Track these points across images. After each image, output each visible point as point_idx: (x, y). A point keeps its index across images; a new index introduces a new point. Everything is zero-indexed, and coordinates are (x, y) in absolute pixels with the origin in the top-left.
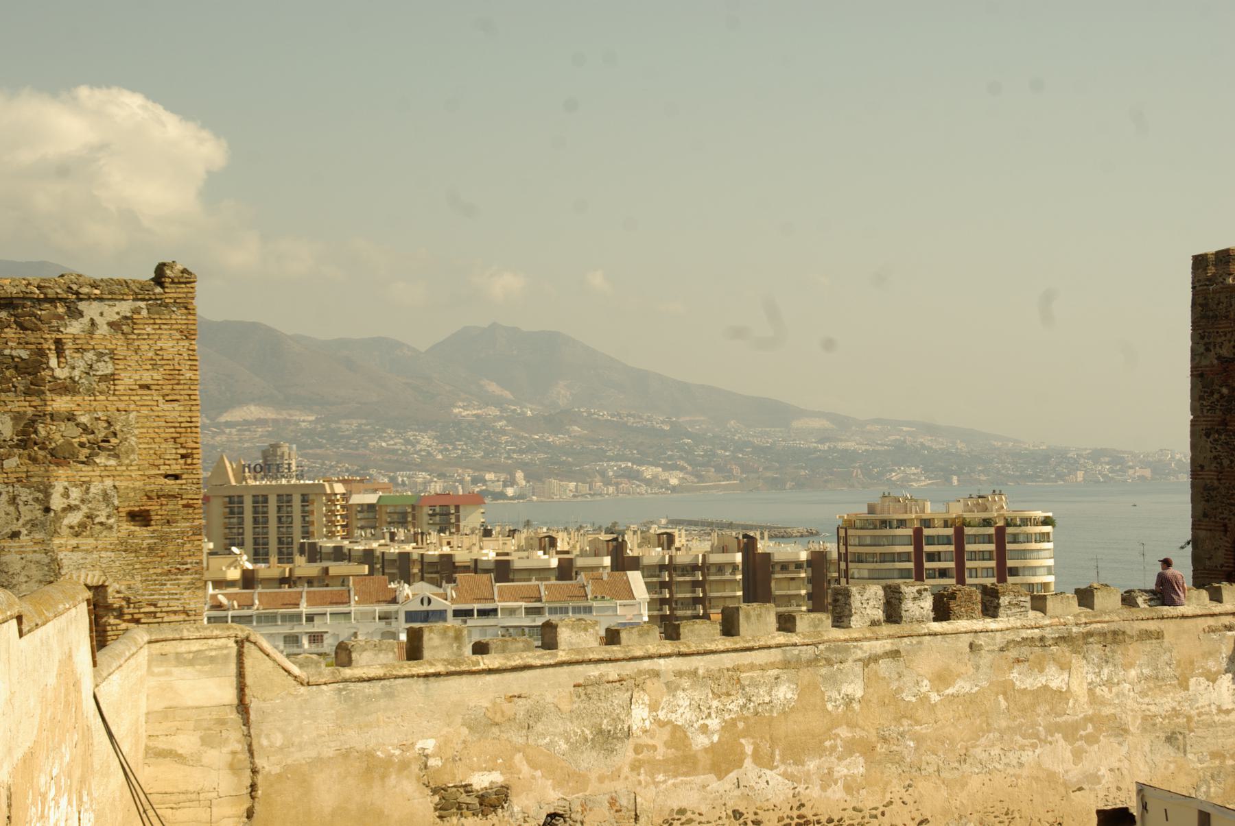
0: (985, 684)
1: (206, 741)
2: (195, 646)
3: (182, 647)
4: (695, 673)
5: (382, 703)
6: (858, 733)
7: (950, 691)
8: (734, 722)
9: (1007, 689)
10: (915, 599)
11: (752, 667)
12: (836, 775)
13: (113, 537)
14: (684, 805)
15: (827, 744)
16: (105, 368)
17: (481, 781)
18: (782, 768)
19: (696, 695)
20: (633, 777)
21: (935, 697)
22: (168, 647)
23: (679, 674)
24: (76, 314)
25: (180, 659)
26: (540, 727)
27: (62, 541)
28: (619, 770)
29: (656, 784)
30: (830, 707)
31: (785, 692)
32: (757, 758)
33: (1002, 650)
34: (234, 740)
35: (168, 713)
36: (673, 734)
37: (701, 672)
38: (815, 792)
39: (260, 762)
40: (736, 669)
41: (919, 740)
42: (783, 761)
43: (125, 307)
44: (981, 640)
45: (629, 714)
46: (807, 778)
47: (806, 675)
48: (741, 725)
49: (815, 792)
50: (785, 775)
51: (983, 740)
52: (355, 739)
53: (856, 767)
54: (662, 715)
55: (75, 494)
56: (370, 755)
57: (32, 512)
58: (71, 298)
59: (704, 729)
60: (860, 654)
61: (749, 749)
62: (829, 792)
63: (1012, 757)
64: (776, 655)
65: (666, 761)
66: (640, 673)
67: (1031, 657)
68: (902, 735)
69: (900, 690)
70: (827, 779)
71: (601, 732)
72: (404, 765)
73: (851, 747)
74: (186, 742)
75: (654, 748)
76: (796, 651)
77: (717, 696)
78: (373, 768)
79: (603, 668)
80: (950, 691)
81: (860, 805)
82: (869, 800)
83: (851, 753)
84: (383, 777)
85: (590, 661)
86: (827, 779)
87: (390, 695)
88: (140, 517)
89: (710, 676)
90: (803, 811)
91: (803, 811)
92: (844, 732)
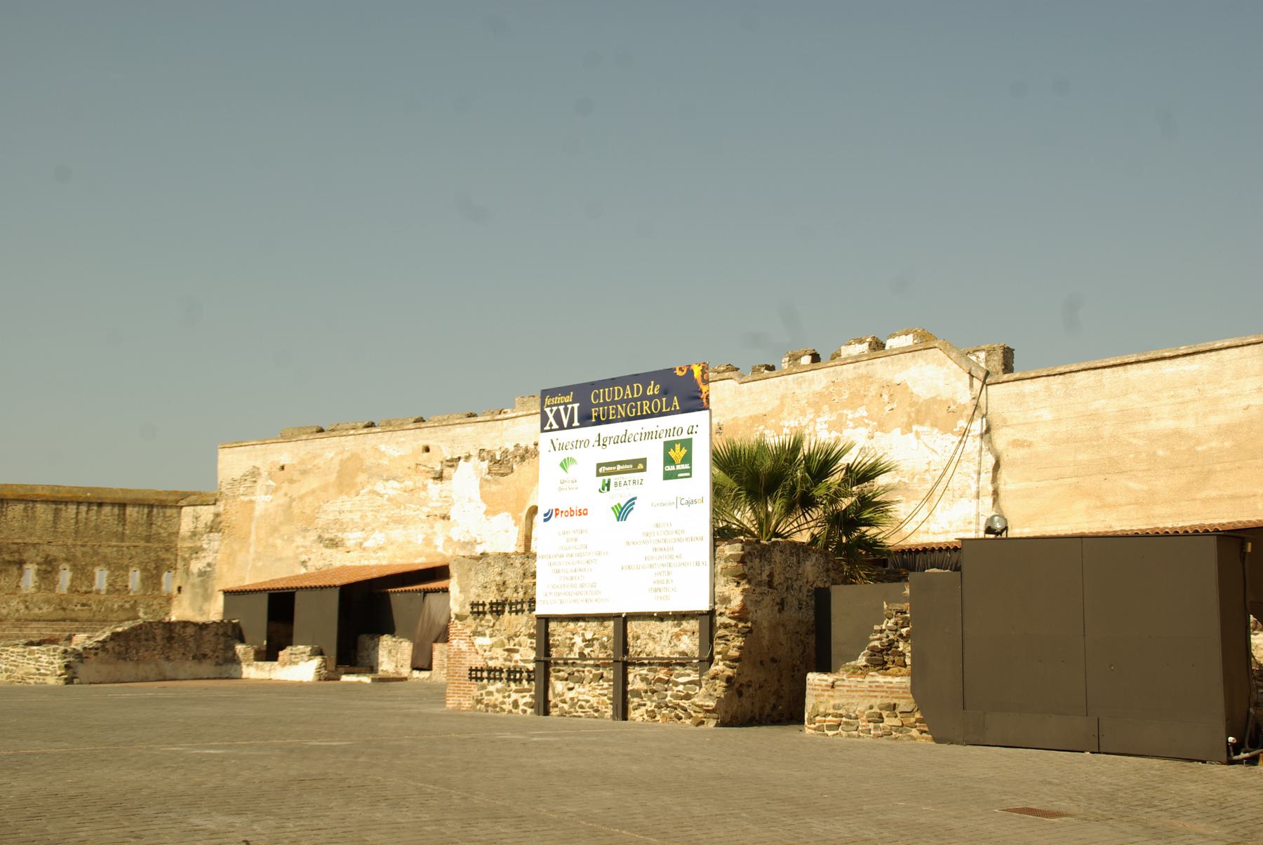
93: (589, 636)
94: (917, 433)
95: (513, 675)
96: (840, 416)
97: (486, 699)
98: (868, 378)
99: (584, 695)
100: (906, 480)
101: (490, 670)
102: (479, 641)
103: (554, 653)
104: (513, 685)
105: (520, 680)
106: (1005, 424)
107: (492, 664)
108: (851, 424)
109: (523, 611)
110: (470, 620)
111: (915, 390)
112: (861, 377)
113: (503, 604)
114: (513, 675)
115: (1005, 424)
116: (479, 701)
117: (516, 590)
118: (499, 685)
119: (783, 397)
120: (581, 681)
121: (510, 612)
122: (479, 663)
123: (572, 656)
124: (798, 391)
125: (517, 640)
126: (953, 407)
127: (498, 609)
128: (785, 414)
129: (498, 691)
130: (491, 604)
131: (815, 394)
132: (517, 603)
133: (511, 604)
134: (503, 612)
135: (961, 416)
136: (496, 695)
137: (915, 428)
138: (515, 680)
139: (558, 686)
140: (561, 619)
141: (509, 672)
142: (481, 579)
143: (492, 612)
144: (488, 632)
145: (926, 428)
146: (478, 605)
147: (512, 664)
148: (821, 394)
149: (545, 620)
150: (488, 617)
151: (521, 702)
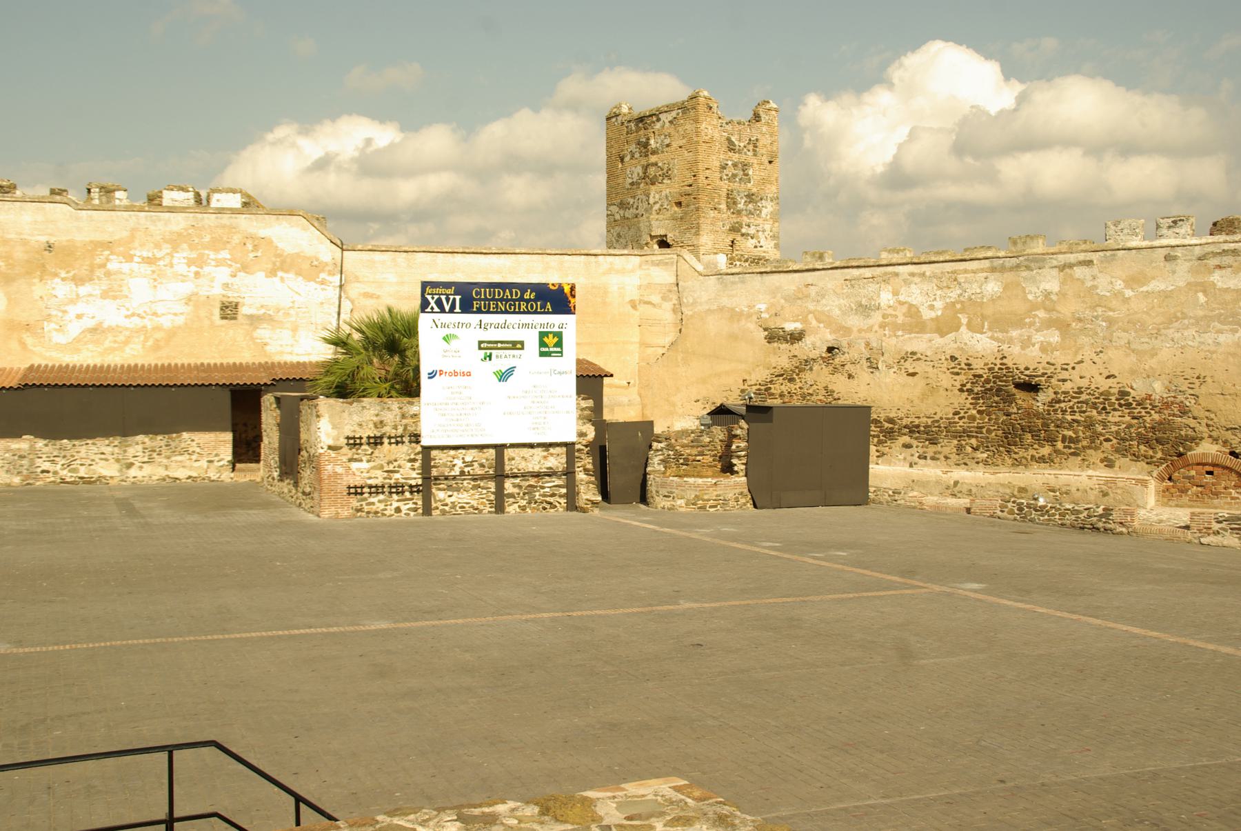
0: (1182, 284)
1: (664, 298)
2: (660, 258)
3: (654, 258)
4: (924, 274)
5: (739, 285)
6: (1054, 315)
7: (1145, 289)
8: (953, 304)
9: (1205, 288)
10: (1170, 227)
11: (966, 271)
12: (1033, 341)
13: (668, 214)
14: (915, 350)
15: (1027, 320)
16: (667, 141)
17: (790, 326)
18: (990, 334)
19: (925, 287)
20: (881, 332)
21: (1129, 293)
22: (648, 258)
23: (912, 275)
24: (658, 120)
25: (654, 264)
26: (824, 301)
27: (654, 216)
28: (872, 327)
29: (897, 337)
30: (1030, 297)
31: (993, 287)
32: (970, 327)
33: (1199, 259)
34: (674, 297)
35: (649, 285)
36: (909, 309)
37: (928, 274)
38: (1016, 349)
39: (684, 309)
40: (954, 272)
41: (1111, 322)
42: (990, 329)
43: (674, 114)
44: (1179, 252)
45: (879, 296)
46: (1011, 341)
47: (1009, 276)
48: (958, 306)
49: (1016, 349)
50: (992, 338)
51: (1176, 324)
52: (725, 302)
53: (1054, 337)
54: (902, 298)
55: (657, 196)
56: (733, 309)
57: (645, 204)
58: (655, 115)
59: (932, 307)
60: (1055, 263)
61: (964, 321)
62: (1028, 351)
63: (1209, 338)
64: (986, 263)
65: (903, 324)
66: (886, 274)
67: (1235, 264)
68: (1096, 317)
69: (1096, 287)
70: (1026, 343)
71: (861, 305)
72: (749, 316)
73: (1049, 324)
74: (656, 299)
75: (896, 316)
76: (1001, 261)
77: (939, 288)
78: (734, 315)
79: (862, 271)
80: (1145, 289)
81: (1052, 361)
82: (1059, 358)
83: (1048, 327)
84: (739, 321)
85: (852, 267)
86: (1026, 343)
87: (743, 282)
88: (679, 204)
89: (935, 276)
90: (1005, 361)
91: (1005, 361)
92: (1041, 314)
93: (468, 459)
94: (282, 278)
95: (398, 489)
96: (201, 256)
97: (366, 508)
98: (232, 229)
99: (463, 500)
100: (271, 312)
101: (370, 487)
102: (354, 465)
103: (434, 472)
104: (395, 497)
105: (403, 492)
106: (357, 280)
107: (370, 482)
108: (213, 263)
109: (403, 443)
110: (345, 450)
111: (280, 245)
112: (224, 226)
113: (381, 437)
114: (398, 489)
115: (357, 280)
116: (358, 510)
117: (395, 428)
118: (381, 497)
119: (134, 230)
120: (458, 490)
121: (390, 443)
122: (358, 481)
123: (453, 473)
124: (152, 228)
125: (396, 464)
126: (315, 263)
127: (376, 441)
128: (136, 244)
129: (380, 501)
130: (369, 438)
131: (171, 233)
132: (396, 437)
133: (390, 438)
134: (382, 444)
135: (323, 271)
136: (378, 505)
137: (280, 274)
138: (397, 493)
139: (440, 495)
140: (442, 448)
141: (391, 487)
142: (356, 418)
143: (369, 444)
144: (364, 458)
145: (291, 275)
146: (354, 438)
147: (392, 482)
148: (179, 234)
149: (427, 450)
150: (365, 447)
151: (404, 508)
